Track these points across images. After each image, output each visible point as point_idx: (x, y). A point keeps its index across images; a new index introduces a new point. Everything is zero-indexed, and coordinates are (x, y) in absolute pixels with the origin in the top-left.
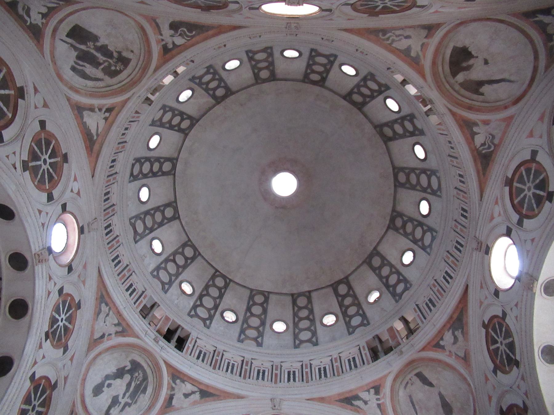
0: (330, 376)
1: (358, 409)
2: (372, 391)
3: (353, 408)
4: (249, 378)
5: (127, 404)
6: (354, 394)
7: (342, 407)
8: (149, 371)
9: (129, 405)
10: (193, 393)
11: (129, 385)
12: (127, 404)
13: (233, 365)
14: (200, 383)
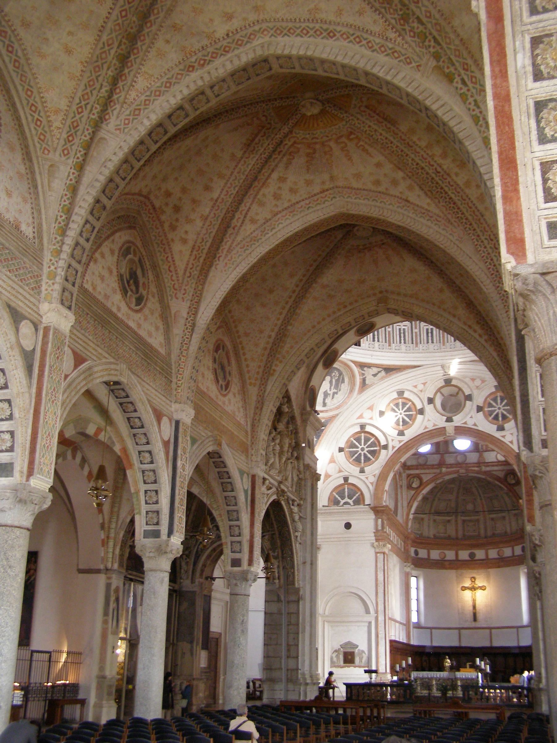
5: (334, 393)
8: (341, 369)
9: (336, 393)
10: (379, 372)
11: (331, 382)
12: (334, 393)
13: (404, 329)
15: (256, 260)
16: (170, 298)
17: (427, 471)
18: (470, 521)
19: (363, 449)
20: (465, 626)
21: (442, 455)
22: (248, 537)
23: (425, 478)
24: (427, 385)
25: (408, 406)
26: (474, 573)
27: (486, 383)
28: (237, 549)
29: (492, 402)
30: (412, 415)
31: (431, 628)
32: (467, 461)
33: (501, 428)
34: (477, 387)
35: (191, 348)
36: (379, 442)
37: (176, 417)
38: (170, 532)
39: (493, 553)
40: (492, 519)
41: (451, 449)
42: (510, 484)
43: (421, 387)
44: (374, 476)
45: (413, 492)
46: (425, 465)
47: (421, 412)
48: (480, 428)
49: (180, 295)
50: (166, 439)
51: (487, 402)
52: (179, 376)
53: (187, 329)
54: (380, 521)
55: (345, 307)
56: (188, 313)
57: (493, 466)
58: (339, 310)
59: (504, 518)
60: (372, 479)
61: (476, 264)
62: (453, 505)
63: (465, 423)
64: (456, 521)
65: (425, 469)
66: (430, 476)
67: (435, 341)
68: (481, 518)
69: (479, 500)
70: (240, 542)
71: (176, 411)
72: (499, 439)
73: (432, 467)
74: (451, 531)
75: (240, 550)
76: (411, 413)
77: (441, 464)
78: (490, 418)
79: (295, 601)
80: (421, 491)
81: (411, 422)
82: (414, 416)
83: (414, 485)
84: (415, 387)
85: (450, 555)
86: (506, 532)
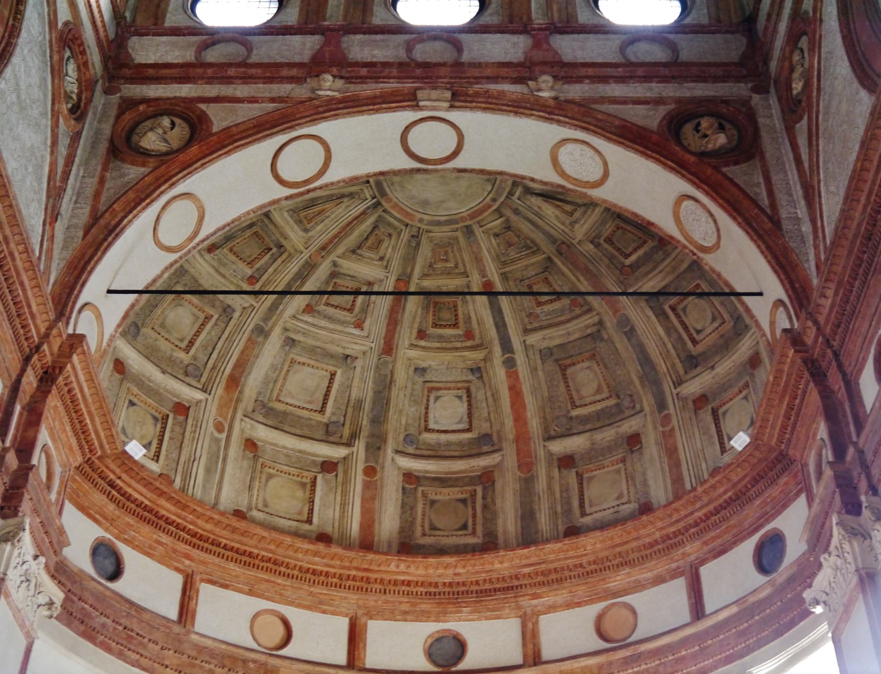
17: (241, 90)
18: (442, 481)
40: (567, 461)
42: (703, 154)
45: (134, 172)
57: (604, 79)
59: (634, 441)
64: (370, 471)
65: (228, 80)
69: (499, 374)
83: (151, 141)
86: (646, 508)
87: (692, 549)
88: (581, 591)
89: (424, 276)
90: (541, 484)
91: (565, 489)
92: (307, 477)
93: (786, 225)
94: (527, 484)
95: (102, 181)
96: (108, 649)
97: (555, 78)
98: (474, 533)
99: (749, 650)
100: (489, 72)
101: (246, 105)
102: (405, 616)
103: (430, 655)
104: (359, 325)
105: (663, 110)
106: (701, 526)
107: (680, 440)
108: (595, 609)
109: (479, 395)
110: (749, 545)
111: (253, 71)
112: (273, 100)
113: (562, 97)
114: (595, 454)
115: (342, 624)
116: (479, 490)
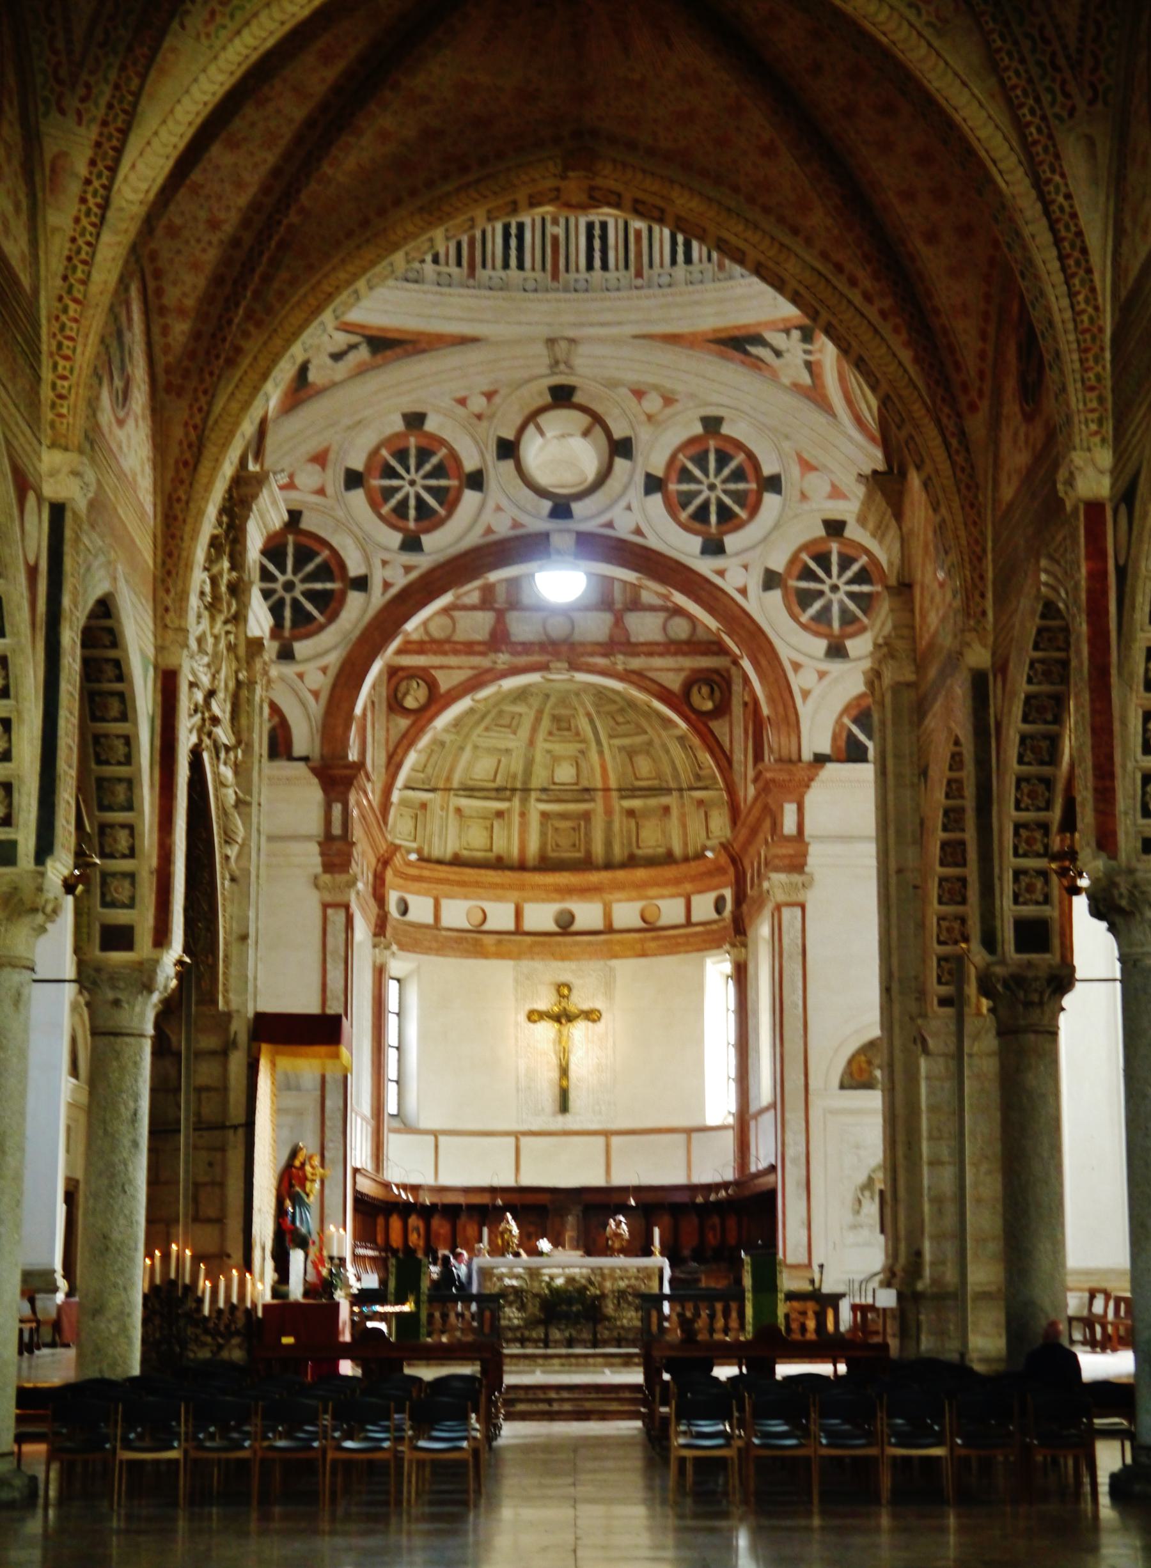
0: (701, 260)
1: (760, 364)
2: (796, 334)
3: (748, 360)
4: (484, 266)
6: (752, 331)
7: (723, 356)
10: (352, 347)
14: (363, 327)
15: (306, 12)
16: (42, 108)
17: (452, 660)
18: (563, 816)
19: (289, 586)
20: (535, 1127)
21: (500, 615)
22: (154, 862)
23: (446, 682)
24: (497, 400)
25: (434, 460)
26: (563, 971)
27: (677, 407)
28: (123, 895)
29: (690, 466)
30: (446, 489)
31: (435, 1134)
32: (577, 637)
33: (714, 548)
34: (650, 417)
35: (97, 277)
36: (343, 566)
37: (50, 490)
38: (44, 849)
39: (627, 913)
40: (631, 813)
41: (526, 600)
42: (700, 714)
43: (478, 403)
44: (324, 670)
45: (404, 723)
46: (448, 641)
47: (476, 481)
48: (653, 542)
49: (72, 102)
50: (32, 561)
51: (678, 465)
52: (62, 363)
53: (88, 213)
54: (337, 808)
55: (465, 169)
56: (93, 163)
57: (651, 654)
58: (445, 177)
59: (666, 810)
60: (318, 680)
61: (981, 105)
62: (516, 765)
63: (610, 525)
64: (523, 815)
66: (459, 677)
67: (528, 263)
68: (597, 807)
70: (131, 876)
71: (53, 473)
72: (707, 581)
73: (469, 648)
74: (506, 843)
75: (132, 898)
76: (443, 482)
77: (498, 639)
78: (684, 516)
79: (213, 1053)
80: (432, 719)
81: (442, 512)
82: (452, 495)
83: (410, 703)
84: (462, 402)
85: (500, 916)
87: (688, 887)
88: (634, 894)
89: (553, 708)
90: (616, 826)
91: (629, 831)
92: (488, 823)
93: (735, 765)
94: (609, 825)
95: (388, 730)
96: (409, 951)
97: (625, 654)
98: (579, 851)
99: (706, 949)
100: (589, 649)
101: (458, 671)
102: (543, 901)
103: (557, 923)
104: (515, 733)
105: (682, 676)
106: (693, 879)
107: (689, 823)
108: (639, 905)
109: (583, 764)
110: (711, 897)
111: (459, 647)
112: (472, 668)
113: (628, 667)
114: (646, 813)
115: (510, 908)
116: (582, 823)
